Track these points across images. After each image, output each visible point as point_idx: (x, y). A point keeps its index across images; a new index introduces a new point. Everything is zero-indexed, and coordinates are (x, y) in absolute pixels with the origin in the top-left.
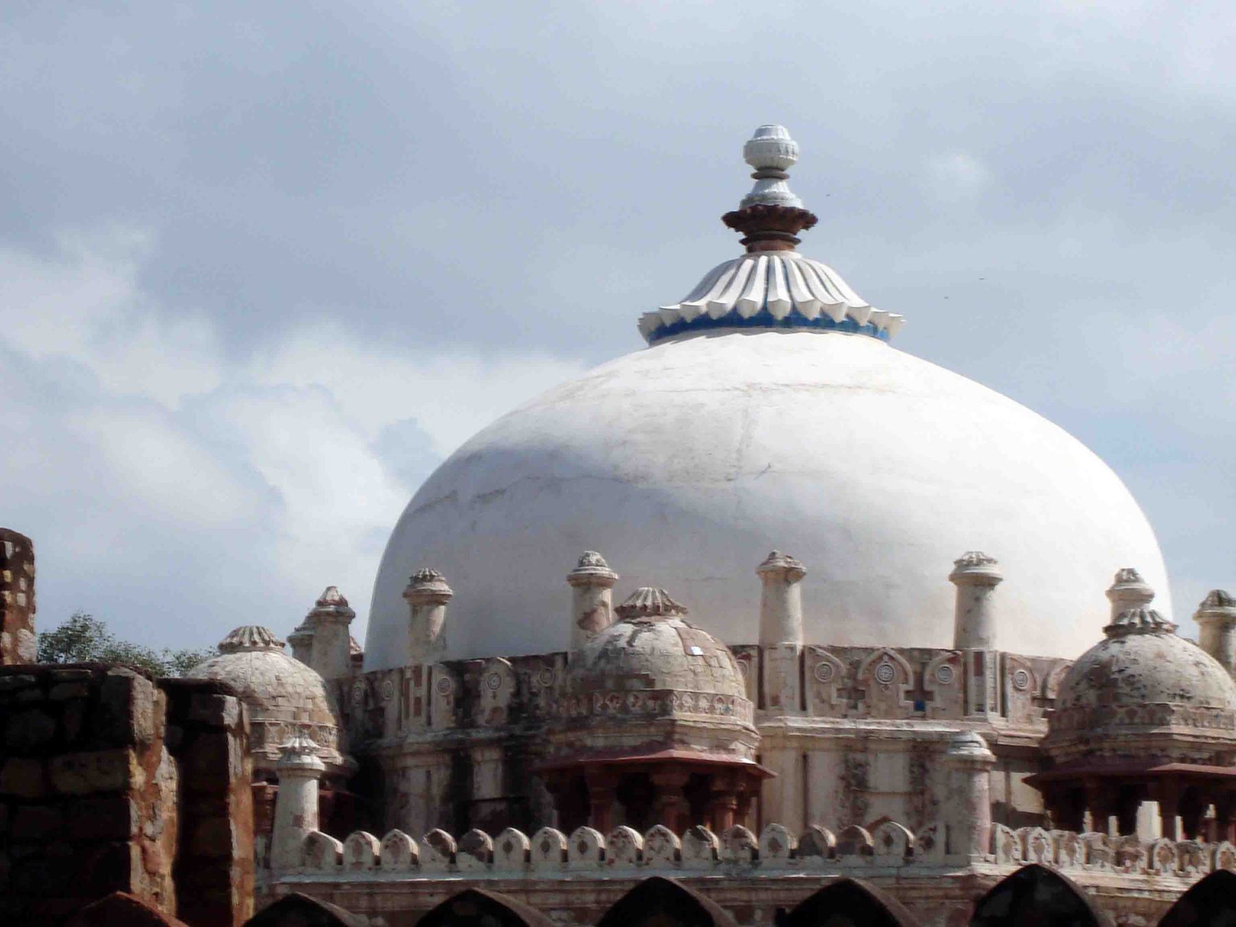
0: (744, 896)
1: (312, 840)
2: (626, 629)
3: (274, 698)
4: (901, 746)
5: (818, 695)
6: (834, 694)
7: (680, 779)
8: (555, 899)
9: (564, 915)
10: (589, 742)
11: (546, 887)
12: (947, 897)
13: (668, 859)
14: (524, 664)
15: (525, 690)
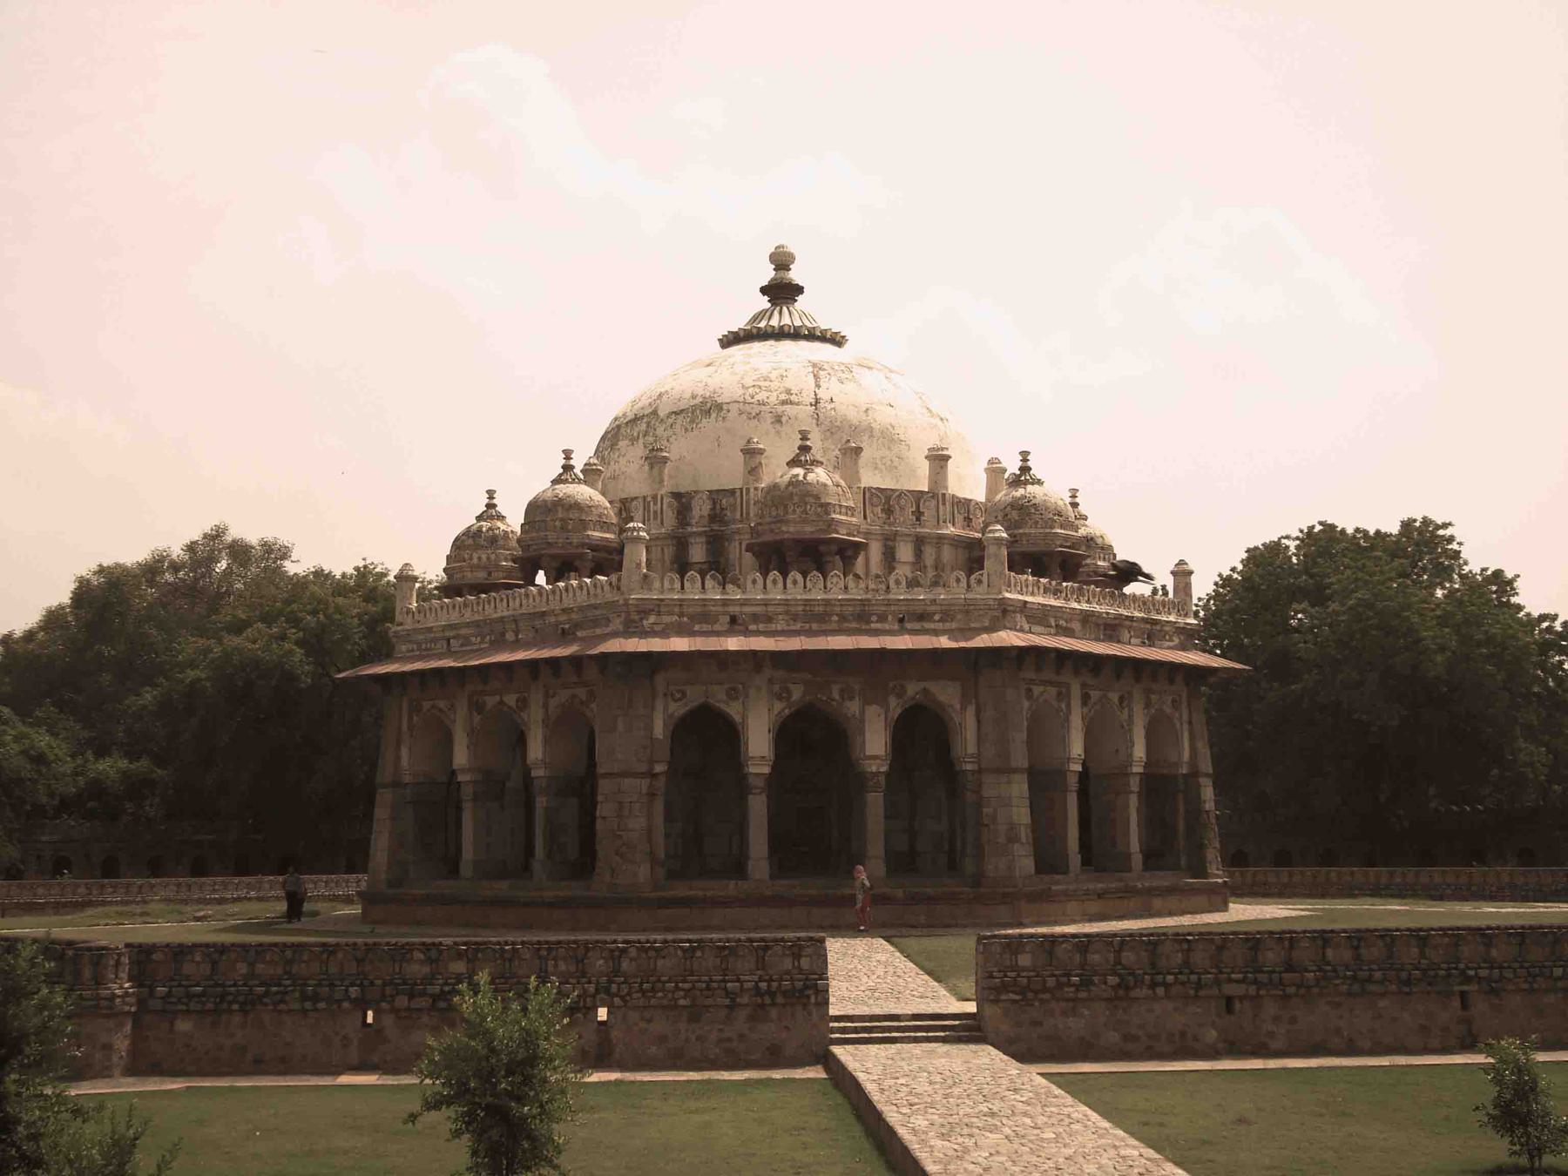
0: (883, 608)
1: (646, 576)
2: (799, 471)
3: (590, 507)
4: (911, 539)
5: (873, 512)
6: (880, 512)
7: (834, 548)
8: (780, 609)
9: (786, 618)
10: (784, 529)
11: (777, 602)
12: (990, 609)
13: (841, 589)
14: (715, 495)
15: (718, 507)
